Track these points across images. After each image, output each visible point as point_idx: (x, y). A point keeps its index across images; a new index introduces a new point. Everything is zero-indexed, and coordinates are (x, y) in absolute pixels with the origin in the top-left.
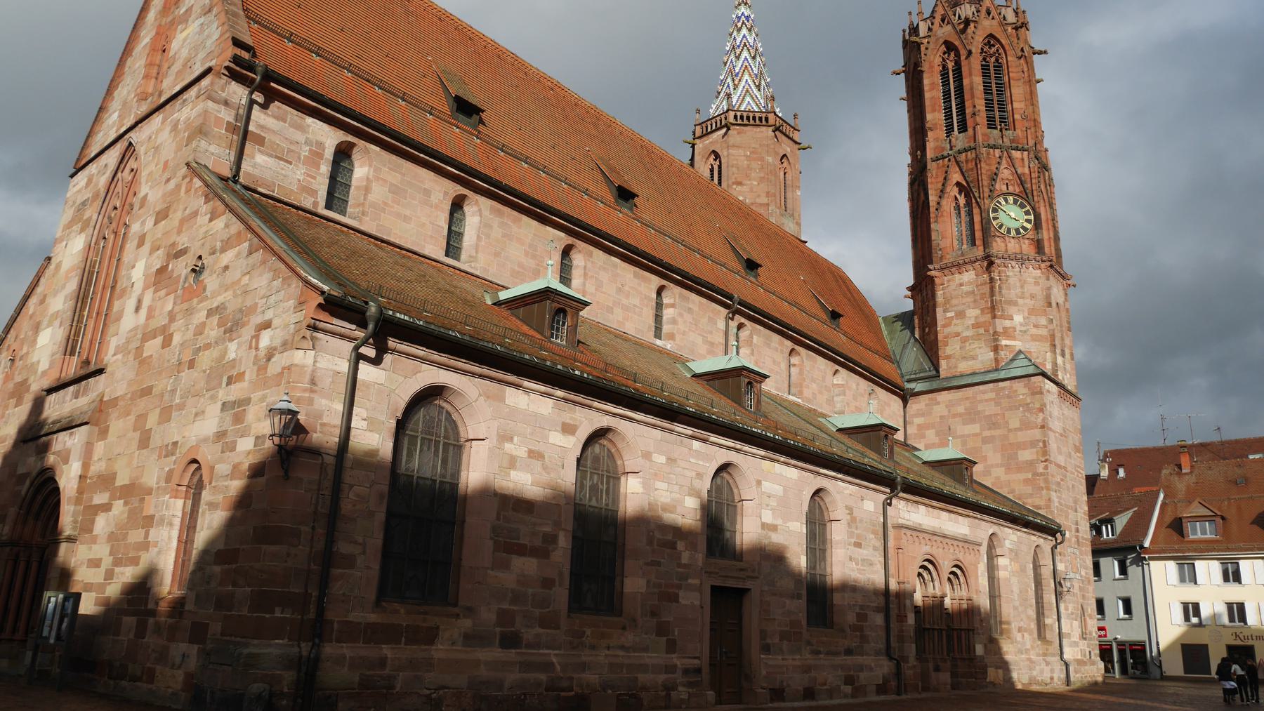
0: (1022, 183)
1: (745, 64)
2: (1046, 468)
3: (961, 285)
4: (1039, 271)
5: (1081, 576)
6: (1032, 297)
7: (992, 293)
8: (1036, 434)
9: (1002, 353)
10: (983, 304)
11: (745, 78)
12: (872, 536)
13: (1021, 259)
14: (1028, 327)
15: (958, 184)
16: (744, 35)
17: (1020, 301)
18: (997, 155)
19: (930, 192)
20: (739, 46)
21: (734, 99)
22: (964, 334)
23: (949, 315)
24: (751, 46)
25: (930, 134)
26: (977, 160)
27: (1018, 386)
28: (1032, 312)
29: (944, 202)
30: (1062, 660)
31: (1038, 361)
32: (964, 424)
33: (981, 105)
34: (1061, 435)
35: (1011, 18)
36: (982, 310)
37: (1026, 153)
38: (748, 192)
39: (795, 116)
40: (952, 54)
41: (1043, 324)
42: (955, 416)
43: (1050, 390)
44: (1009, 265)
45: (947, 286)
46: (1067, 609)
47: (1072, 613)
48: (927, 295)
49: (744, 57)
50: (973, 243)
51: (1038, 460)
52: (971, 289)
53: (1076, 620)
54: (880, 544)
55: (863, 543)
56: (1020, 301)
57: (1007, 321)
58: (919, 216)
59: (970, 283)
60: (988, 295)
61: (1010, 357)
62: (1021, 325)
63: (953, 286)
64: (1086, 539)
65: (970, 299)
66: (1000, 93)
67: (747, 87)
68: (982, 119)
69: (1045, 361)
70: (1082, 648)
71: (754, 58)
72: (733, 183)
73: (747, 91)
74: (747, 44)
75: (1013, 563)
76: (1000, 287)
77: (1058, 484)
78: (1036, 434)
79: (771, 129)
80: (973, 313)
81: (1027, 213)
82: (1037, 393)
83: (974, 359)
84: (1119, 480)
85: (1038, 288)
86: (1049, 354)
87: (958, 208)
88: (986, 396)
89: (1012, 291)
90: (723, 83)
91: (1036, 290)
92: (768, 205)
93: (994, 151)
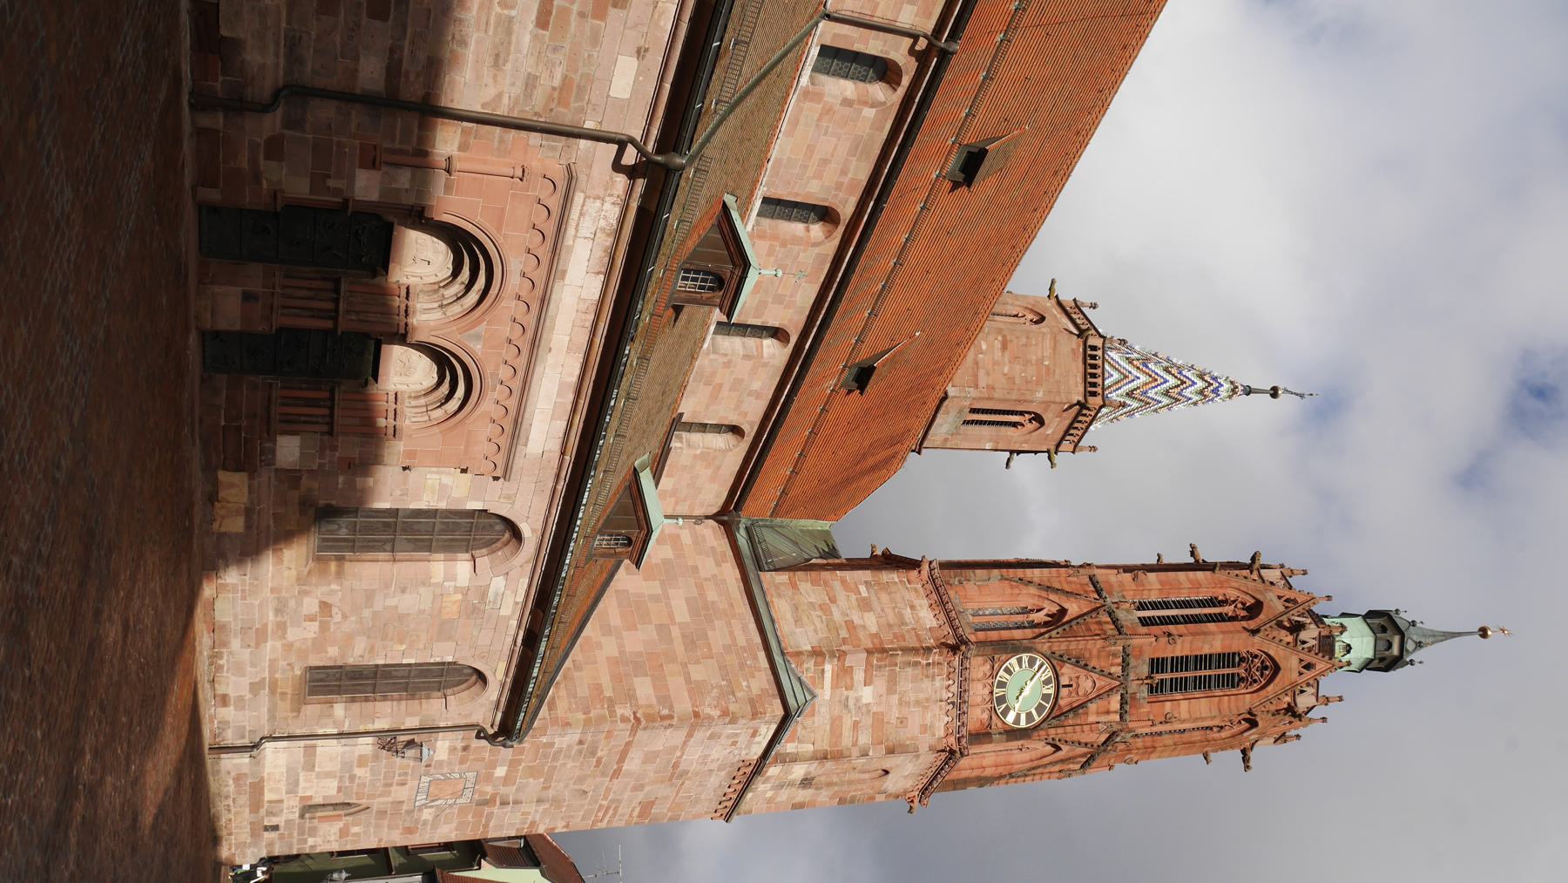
1: (1159, 378)
2: (624, 719)
3: (912, 607)
4: (942, 733)
6: (902, 721)
7: (907, 650)
8: (683, 705)
9: (810, 664)
10: (887, 637)
11: (1141, 376)
13: (960, 704)
14: (853, 712)
15: (1063, 611)
16: (1196, 384)
17: (895, 699)
18: (1113, 670)
20: (1180, 373)
22: (834, 609)
24: (1182, 390)
27: (763, 680)
29: (1032, 590)
30: (261, 739)
31: (799, 728)
32: (687, 600)
33: (1182, 648)
36: (876, 635)
37: (1117, 717)
38: (993, 358)
39: (1093, 449)
40: (1244, 613)
41: (860, 739)
42: (700, 586)
43: (758, 739)
44: (951, 682)
45: (907, 588)
47: (352, 778)
49: (1168, 378)
51: (639, 707)
53: (339, 789)
56: (895, 699)
57: (862, 674)
59: (918, 620)
60: (903, 644)
61: (803, 678)
62: (858, 700)
64: (486, 826)
65: (892, 619)
67: (1131, 377)
70: (285, 805)
72: (1004, 337)
73: (1126, 377)
74: (1184, 386)
75: (459, 597)
78: (683, 705)
79: (1081, 398)
80: (870, 622)
82: (753, 706)
83: (796, 622)
86: (810, 748)
87: (1025, 611)
88: (738, 633)
89: (910, 685)
91: (912, 731)
92: (976, 387)
93: (1119, 665)
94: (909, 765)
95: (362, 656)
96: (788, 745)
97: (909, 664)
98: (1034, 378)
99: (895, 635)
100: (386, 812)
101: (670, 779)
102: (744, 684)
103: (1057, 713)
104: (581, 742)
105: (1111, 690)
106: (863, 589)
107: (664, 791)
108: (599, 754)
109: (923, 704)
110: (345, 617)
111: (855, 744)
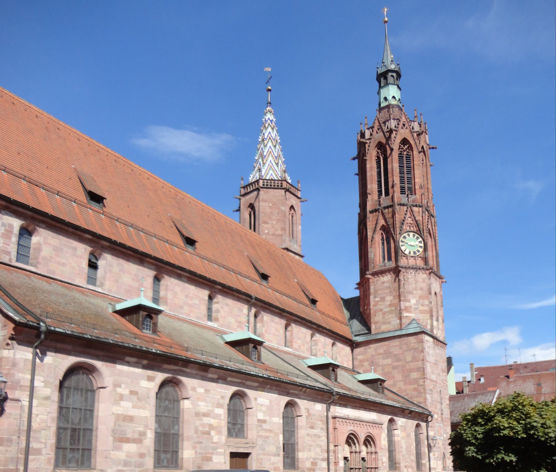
0: (418, 225)
3: (383, 283)
4: (425, 275)
5: (444, 438)
6: (422, 289)
12: (320, 423)
13: (416, 269)
17: (415, 292)
19: (368, 230)
21: (263, 171)
23: (377, 299)
25: (369, 196)
26: (394, 214)
27: (412, 339)
28: (421, 297)
33: (397, 180)
34: (434, 364)
35: (417, 128)
36: (394, 297)
37: (421, 209)
42: (378, 354)
43: (428, 340)
44: (409, 272)
45: (376, 284)
46: (434, 455)
47: (438, 457)
48: (366, 288)
50: (390, 259)
52: (389, 285)
53: (440, 461)
54: (324, 427)
55: (315, 426)
56: (415, 292)
58: (363, 243)
62: (415, 305)
63: (379, 283)
65: (388, 291)
66: (409, 172)
68: (397, 189)
69: (427, 324)
71: (275, 146)
77: (431, 390)
78: (420, 364)
80: (389, 298)
81: (420, 242)
84: (481, 384)
85: (424, 284)
86: (429, 321)
89: (410, 286)
90: (257, 161)
91: (424, 285)
93: (403, 207)
97: (404, 287)
99: (394, 290)
102: (413, 344)
103: (419, 232)
105: (412, 211)
108: (432, 388)
109: (416, 282)
111: (428, 305)
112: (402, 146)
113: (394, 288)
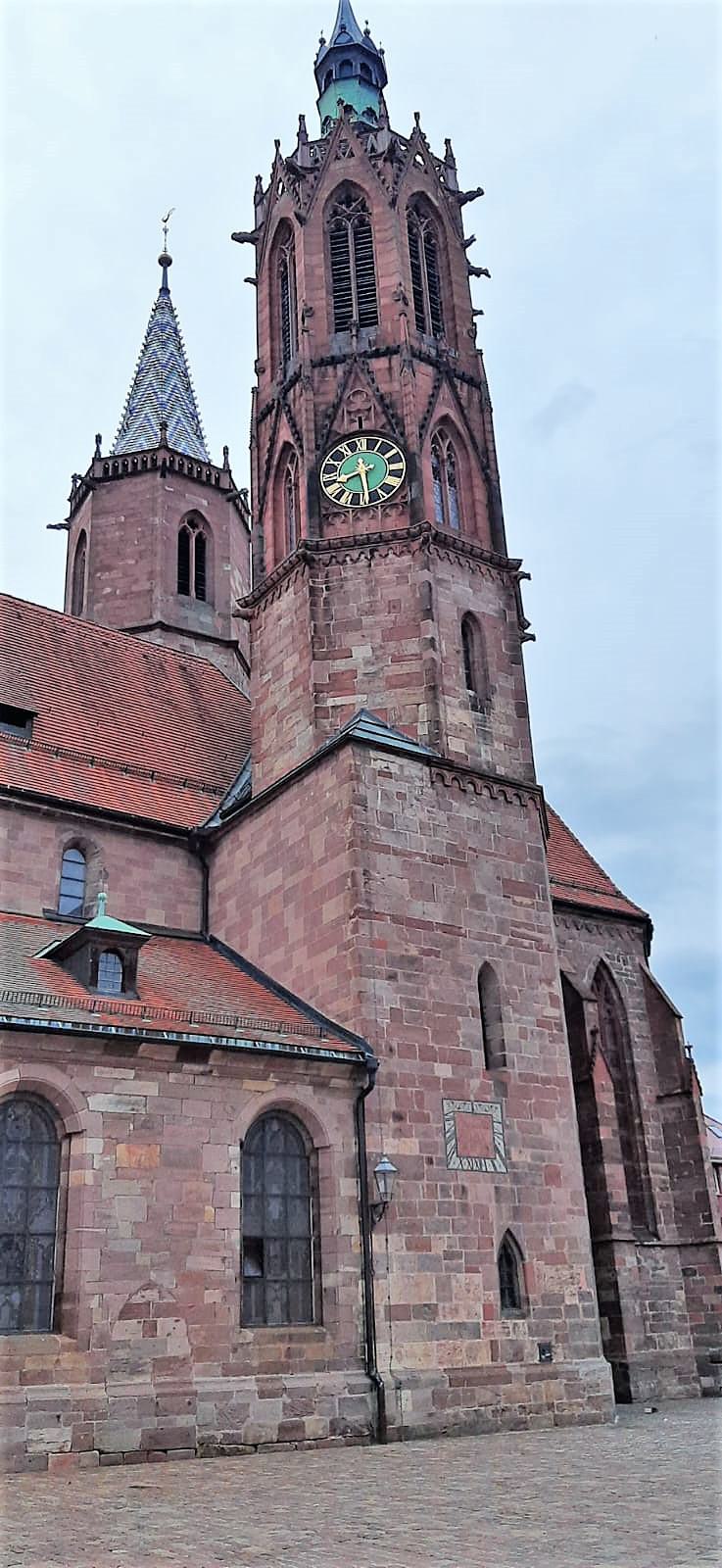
4: (407, 558)
18: (340, 373)
36: (300, 653)
41: (413, 652)
43: (394, 769)
44: (348, 559)
56: (366, 620)
62: (367, 662)
70: (501, 1338)
76: (327, 602)
88: (290, 810)
91: (401, 593)
94: (453, 590)
95: (224, 1259)
96: (419, 733)
98: (140, 529)
100: (515, 1208)
101: (465, 865)
104: (392, 977)
106: (266, 678)
107: (486, 869)
108: (414, 952)
110: (149, 1286)
111: (418, 657)
112: (344, 207)
113: (301, 622)
